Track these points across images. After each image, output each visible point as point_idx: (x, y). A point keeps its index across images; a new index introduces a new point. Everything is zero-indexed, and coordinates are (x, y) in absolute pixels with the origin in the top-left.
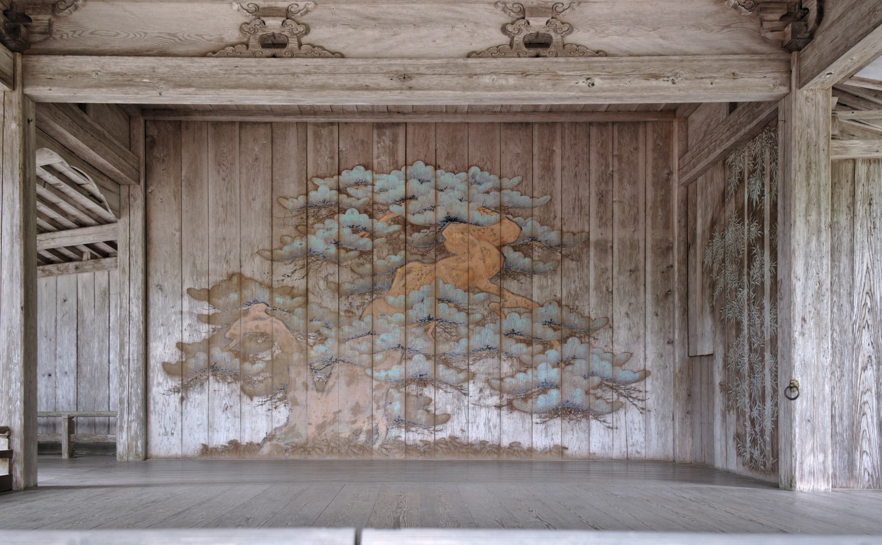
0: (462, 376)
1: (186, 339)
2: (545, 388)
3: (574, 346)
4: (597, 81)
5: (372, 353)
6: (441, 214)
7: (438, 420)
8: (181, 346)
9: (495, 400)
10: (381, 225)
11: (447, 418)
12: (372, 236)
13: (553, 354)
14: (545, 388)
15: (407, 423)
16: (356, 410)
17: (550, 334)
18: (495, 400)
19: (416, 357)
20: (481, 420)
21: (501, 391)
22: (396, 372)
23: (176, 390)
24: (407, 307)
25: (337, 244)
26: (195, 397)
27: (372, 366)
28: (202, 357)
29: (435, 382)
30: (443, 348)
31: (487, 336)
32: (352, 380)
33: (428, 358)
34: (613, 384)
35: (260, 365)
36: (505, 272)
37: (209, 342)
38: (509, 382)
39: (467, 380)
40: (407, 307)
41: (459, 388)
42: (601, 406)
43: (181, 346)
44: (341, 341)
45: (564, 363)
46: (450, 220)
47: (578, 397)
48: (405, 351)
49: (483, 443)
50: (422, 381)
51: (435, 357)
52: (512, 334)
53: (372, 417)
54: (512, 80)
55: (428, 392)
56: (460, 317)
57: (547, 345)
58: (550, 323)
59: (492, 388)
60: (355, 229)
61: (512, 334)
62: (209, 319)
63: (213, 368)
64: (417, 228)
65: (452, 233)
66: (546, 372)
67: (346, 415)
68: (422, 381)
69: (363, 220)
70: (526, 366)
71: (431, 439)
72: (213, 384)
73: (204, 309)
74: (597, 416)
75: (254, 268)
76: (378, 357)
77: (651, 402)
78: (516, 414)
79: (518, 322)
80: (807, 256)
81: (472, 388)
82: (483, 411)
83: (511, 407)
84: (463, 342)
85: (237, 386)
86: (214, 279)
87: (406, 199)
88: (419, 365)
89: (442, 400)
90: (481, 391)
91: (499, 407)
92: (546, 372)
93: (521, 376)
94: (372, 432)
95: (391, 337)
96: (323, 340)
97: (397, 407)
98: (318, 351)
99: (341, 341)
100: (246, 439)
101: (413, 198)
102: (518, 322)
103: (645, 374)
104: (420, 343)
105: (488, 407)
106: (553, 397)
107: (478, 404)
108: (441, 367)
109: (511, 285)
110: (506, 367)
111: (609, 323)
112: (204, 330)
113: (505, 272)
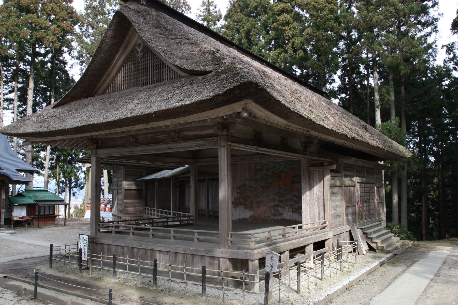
0: (285, 205)
4: (271, 159)
5: (268, 200)
9: (291, 210)
11: (282, 214)
15: (274, 215)
18: (291, 210)
19: (276, 201)
20: (289, 215)
21: (293, 208)
22: (272, 204)
23: (234, 207)
26: (238, 209)
27: (268, 203)
28: (238, 200)
29: (280, 207)
33: (278, 201)
35: (248, 202)
38: (294, 206)
39: (286, 206)
41: (284, 208)
44: (262, 197)
46: (282, 171)
48: (274, 200)
49: (289, 220)
51: (280, 201)
53: (268, 214)
54: (259, 159)
55: (279, 208)
59: (291, 207)
62: (239, 193)
63: (241, 204)
68: (277, 206)
71: (279, 218)
72: (240, 206)
73: (239, 191)
75: (247, 183)
76: (269, 201)
78: (296, 213)
80: (304, 188)
82: (289, 213)
83: (295, 212)
84: (285, 198)
85: (244, 207)
87: (273, 168)
88: (277, 202)
89: (281, 210)
90: (289, 208)
91: (292, 212)
93: (296, 205)
94: (268, 217)
96: (259, 197)
97: (273, 211)
98: (258, 199)
99: (262, 197)
100: (246, 217)
101: (275, 167)
105: (290, 212)
107: (288, 211)
108: (281, 203)
110: (293, 203)
112: (239, 195)
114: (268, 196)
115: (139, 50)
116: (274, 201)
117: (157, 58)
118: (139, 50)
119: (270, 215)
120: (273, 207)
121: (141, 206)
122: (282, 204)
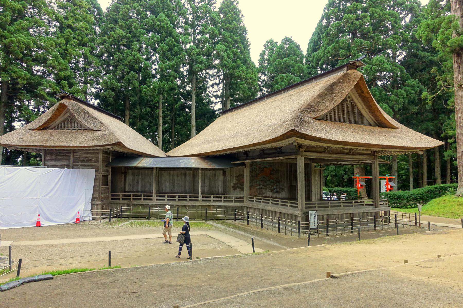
1: (235, 183)
2: (275, 189)
3: (278, 184)
6: (264, 166)
7: (263, 193)
8: (234, 184)
10: (257, 168)
11: (264, 193)
12: (256, 169)
13: (276, 185)
14: (275, 189)
16: (254, 192)
17: (275, 182)
22: (259, 187)
24: (260, 179)
25: (252, 170)
26: (236, 191)
27: (256, 186)
29: (263, 189)
30: (264, 184)
31: (268, 182)
32: (254, 188)
34: (282, 189)
36: (271, 174)
37: (237, 183)
40: (260, 179)
42: (281, 191)
43: (234, 184)
45: (277, 186)
46: (265, 167)
47: (278, 190)
48: (260, 185)
50: (261, 188)
51: (263, 185)
52: (271, 182)
55: (262, 190)
56: (266, 180)
57: (275, 184)
58: (276, 181)
60: (254, 168)
61: (271, 182)
63: (238, 187)
64: (261, 168)
65: (265, 169)
66: (275, 187)
67: (253, 193)
68: (261, 188)
69: (255, 167)
70: (272, 186)
73: (237, 179)
74: (280, 192)
77: (286, 191)
79: (272, 181)
81: (267, 189)
83: (271, 192)
86: (238, 175)
88: (261, 186)
89: (264, 191)
92: (275, 187)
95: (258, 183)
97: (259, 192)
102: (272, 181)
103: (285, 187)
104: (261, 183)
106: (275, 191)
109: (271, 176)
110: (271, 186)
111: (281, 181)
112: (237, 181)
113: (271, 174)
114: (256, 182)
115: (349, 100)
116: (260, 185)
117: (358, 109)
118: (349, 100)
119: (257, 194)
120: (259, 189)
121: (108, 192)
122: (264, 187)
